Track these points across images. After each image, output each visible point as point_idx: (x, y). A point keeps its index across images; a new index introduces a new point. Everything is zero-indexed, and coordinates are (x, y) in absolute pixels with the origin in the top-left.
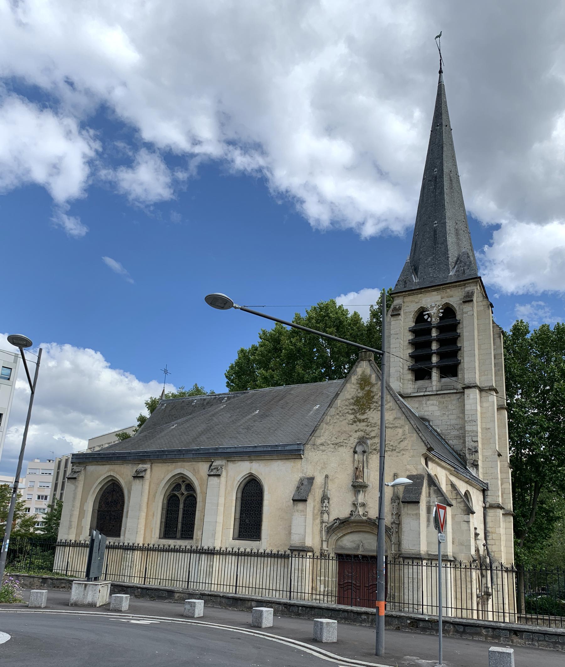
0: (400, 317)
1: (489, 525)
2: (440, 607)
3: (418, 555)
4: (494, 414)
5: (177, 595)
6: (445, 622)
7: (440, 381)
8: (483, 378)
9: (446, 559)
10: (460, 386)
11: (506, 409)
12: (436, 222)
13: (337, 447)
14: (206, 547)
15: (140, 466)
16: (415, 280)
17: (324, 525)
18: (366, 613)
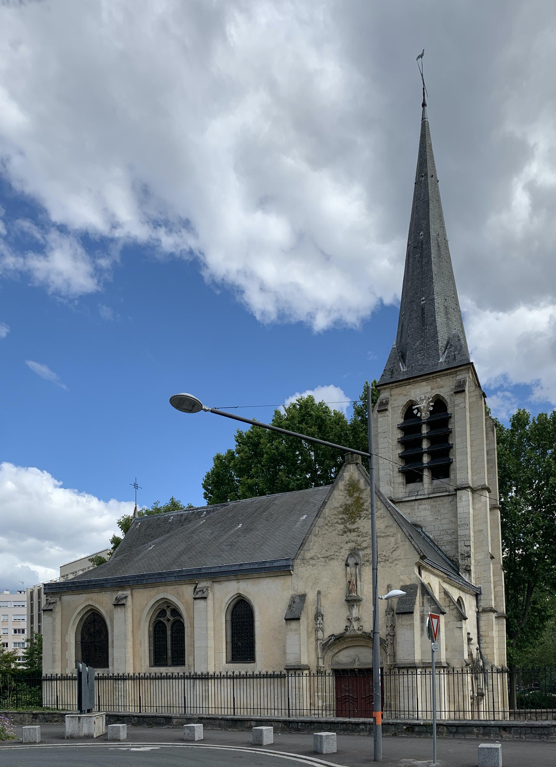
0: (388, 412)
1: (482, 628)
2: (434, 711)
3: (413, 664)
4: (486, 515)
5: (175, 721)
6: (438, 725)
7: (431, 483)
8: (475, 478)
9: (439, 666)
10: (452, 489)
11: (499, 508)
12: (423, 298)
13: (327, 561)
14: (199, 673)
15: (120, 593)
16: (403, 369)
17: (319, 642)
18: (364, 723)
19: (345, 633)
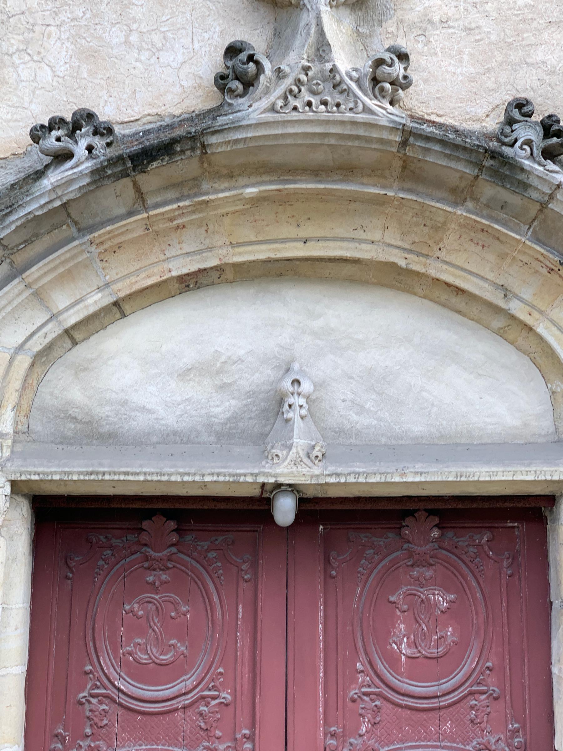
19: (214, 113)
